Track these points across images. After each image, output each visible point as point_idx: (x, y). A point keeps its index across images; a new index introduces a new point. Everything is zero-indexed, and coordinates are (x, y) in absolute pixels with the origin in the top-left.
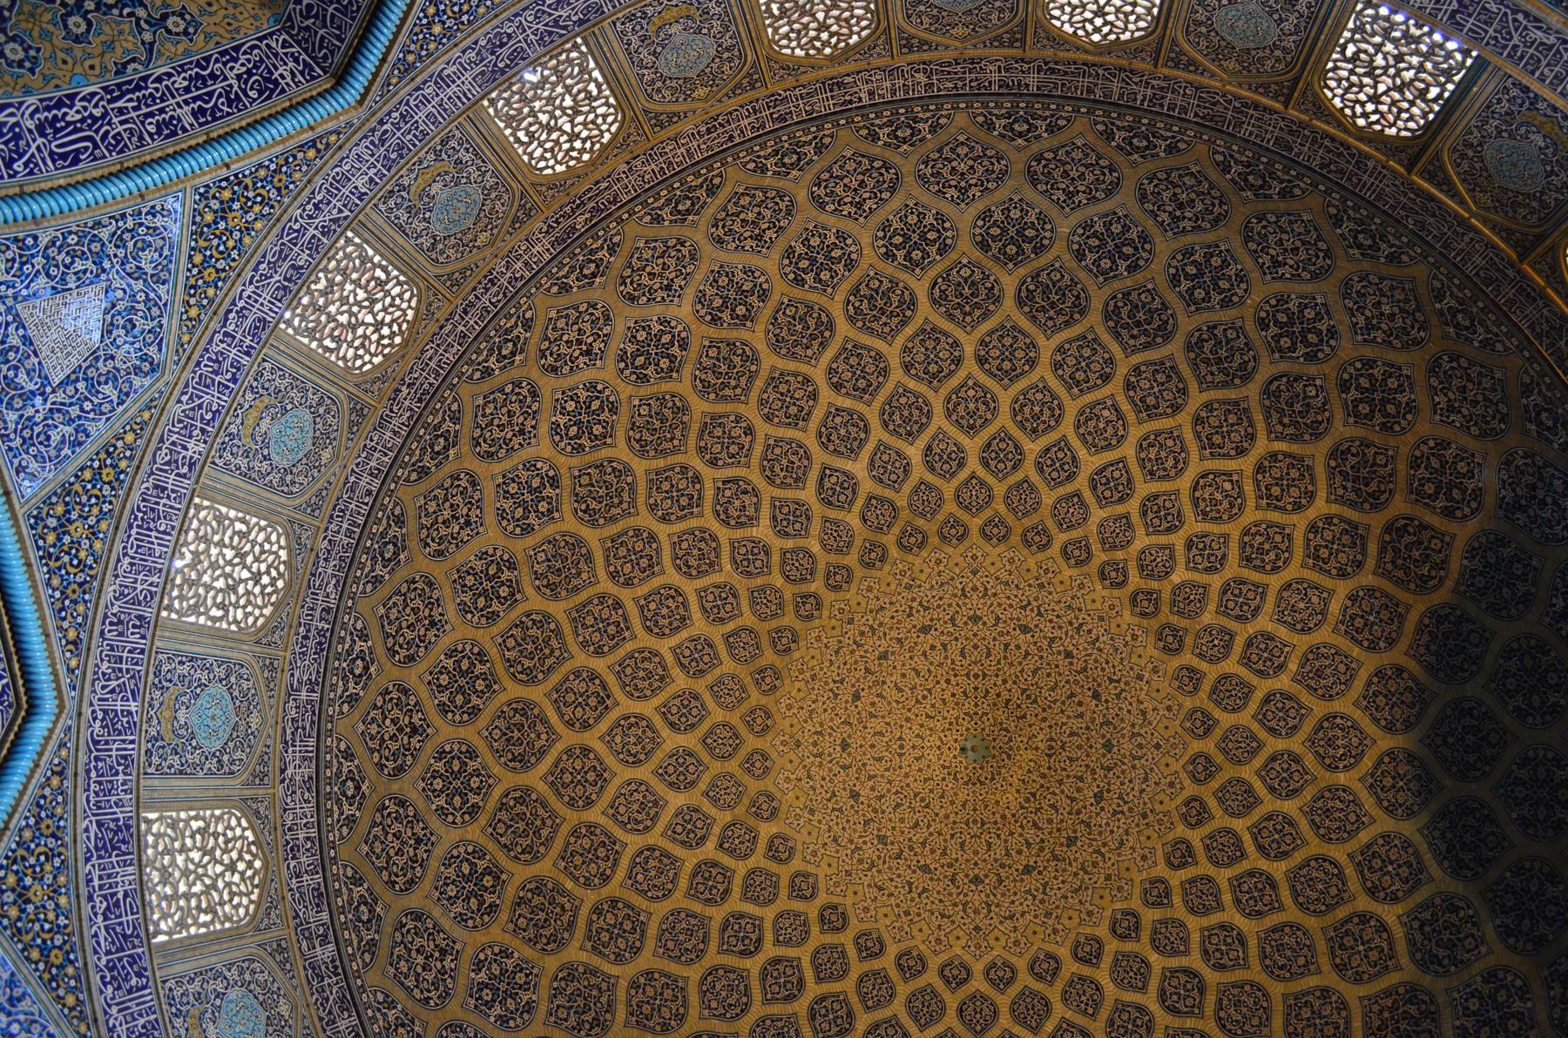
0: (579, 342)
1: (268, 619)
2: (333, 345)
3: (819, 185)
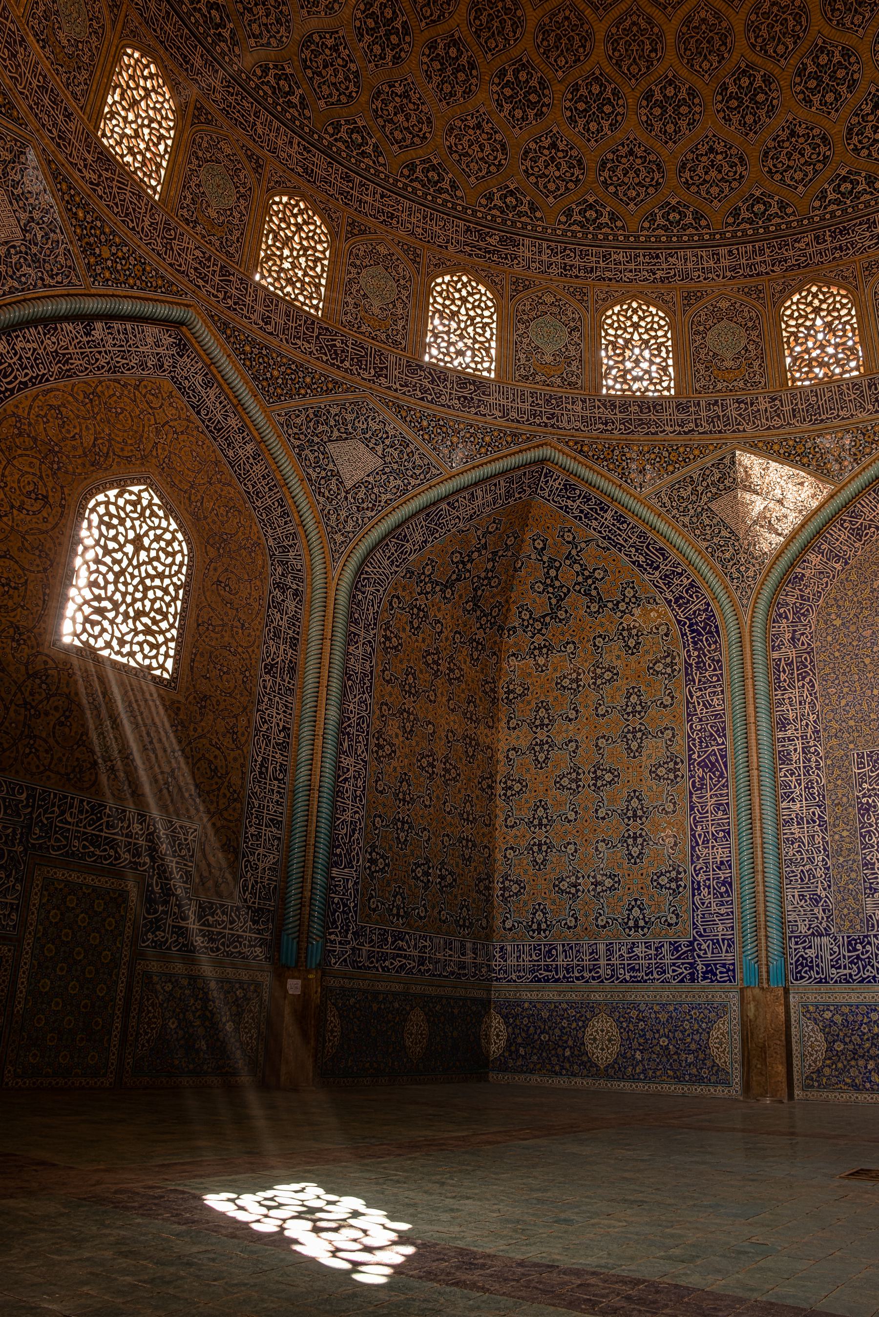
0: (553, 159)
1: (840, 287)
2: (663, 348)
3: (350, 96)
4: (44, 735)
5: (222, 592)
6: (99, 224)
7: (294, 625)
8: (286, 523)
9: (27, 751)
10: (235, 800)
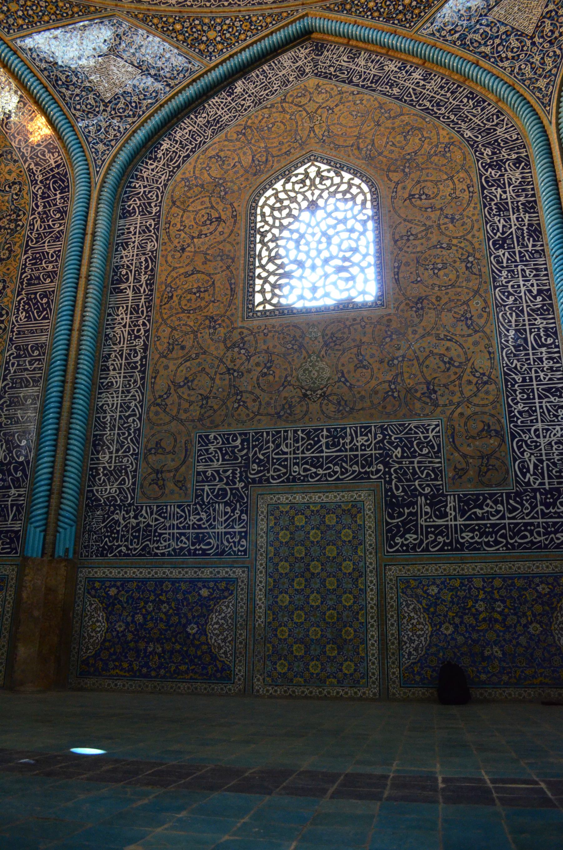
4: (249, 388)
5: (418, 202)
6: (197, 22)
7: (524, 190)
8: (483, 109)
9: (236, 405)
10: (486, 383)
